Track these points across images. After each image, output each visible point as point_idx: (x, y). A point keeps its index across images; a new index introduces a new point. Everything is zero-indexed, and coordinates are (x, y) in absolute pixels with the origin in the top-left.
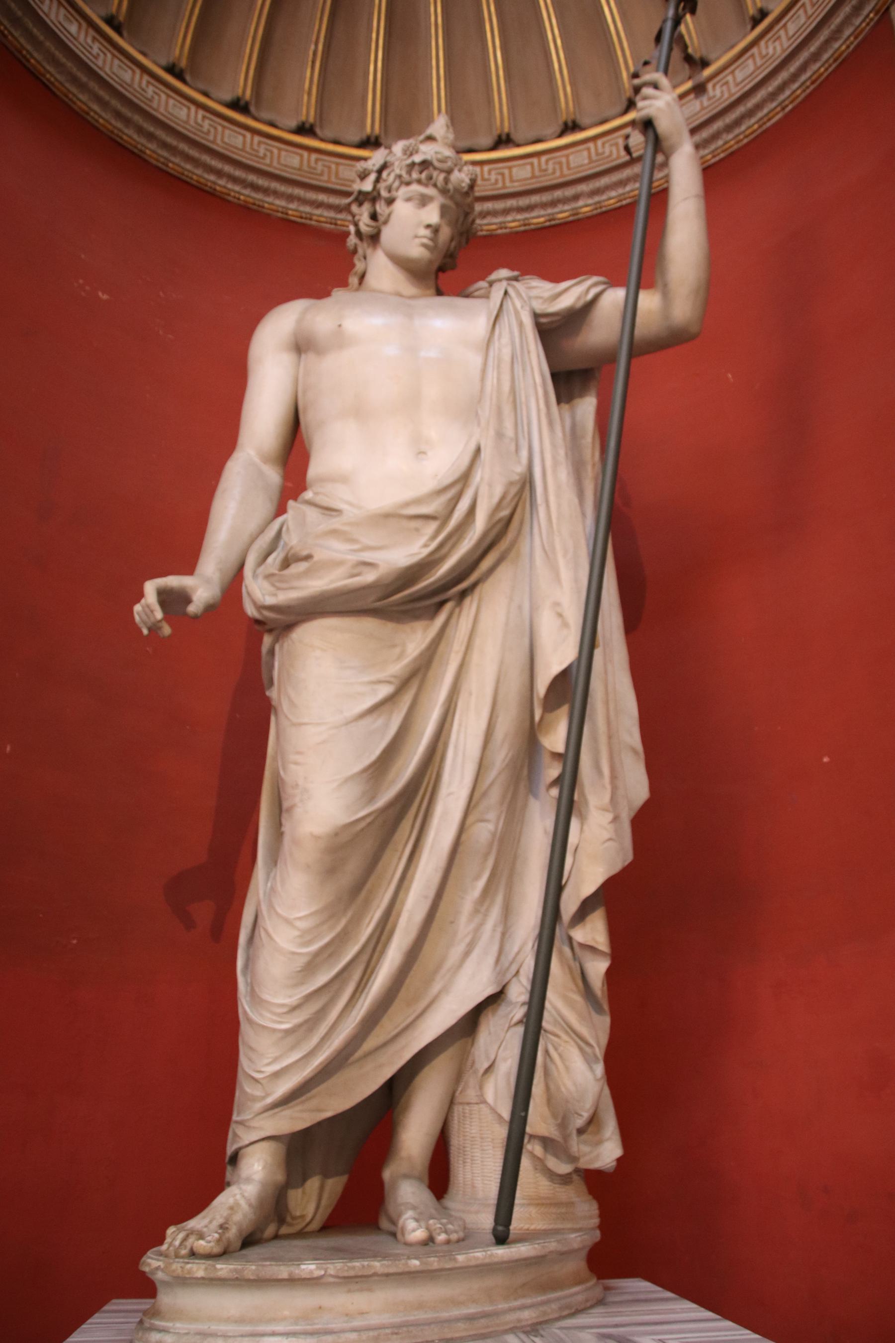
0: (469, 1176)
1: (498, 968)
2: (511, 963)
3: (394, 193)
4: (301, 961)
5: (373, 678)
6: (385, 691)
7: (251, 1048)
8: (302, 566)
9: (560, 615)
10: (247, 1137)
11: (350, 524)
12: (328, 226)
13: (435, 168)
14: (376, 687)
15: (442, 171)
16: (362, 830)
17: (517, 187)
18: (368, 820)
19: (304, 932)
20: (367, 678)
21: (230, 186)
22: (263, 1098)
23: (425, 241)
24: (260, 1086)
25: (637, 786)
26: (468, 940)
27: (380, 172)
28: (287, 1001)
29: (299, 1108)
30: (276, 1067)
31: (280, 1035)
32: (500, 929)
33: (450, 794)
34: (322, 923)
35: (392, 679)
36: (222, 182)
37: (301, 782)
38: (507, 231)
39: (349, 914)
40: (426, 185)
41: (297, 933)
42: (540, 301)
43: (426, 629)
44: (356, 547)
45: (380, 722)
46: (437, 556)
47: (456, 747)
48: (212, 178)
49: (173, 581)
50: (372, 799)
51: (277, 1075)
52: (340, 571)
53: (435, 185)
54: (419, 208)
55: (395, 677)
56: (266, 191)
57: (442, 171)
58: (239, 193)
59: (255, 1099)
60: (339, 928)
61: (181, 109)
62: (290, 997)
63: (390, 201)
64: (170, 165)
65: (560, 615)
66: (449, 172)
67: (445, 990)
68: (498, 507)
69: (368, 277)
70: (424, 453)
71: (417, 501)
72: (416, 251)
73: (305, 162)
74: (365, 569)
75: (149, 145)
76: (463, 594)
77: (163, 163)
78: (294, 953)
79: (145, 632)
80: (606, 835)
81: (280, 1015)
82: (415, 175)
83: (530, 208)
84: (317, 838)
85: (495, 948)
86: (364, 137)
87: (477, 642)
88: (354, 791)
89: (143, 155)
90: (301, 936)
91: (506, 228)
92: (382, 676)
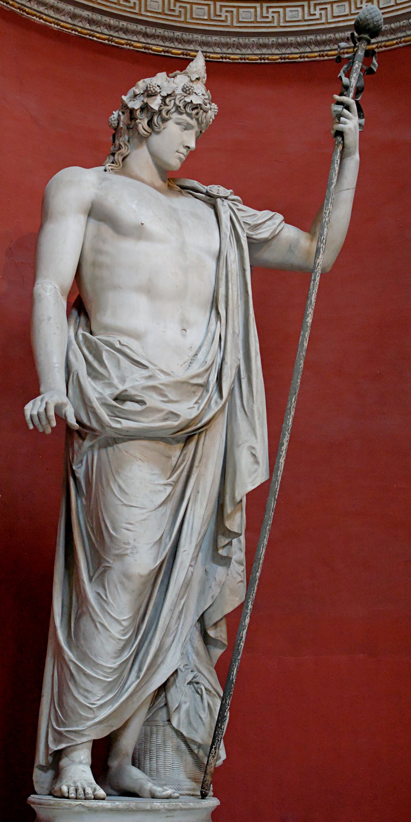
0: (154, 766)
4: (122, 643)
5: (166, 482)
7: (87, 691)
8: (137, 407)
9: (254, 455)
11: (162, 384)
13: (201, 109)
14: (166, 487)
19: (125, 628)
22: (94, 718)
23: (182, 156)
24: (92, 711)
26: (174, 634)
28: (114, 666)
30: (102, 702)
31: (106, 684)
33: (185, 551)
35: (171, 483)
37: (131, 542)
38: (131, 48)
40: (192, 118)
41: (122, 628)
42: (248, 227)
44: (165, 399)
53: (197, 120)
54: (183, 131)
55: (173, 481)
59: (88, 719)
62: (114, 663)
63: (164, 120)
65: (254, 455)
67: (162, 662)
69: (128, 159)
70: (185, 330)
72: (175, 162)
79: (31, 427)
80: (240, 579)
81: (108, 673)
82: (188, 110)
83: (153, 36)
84: (141, 576)
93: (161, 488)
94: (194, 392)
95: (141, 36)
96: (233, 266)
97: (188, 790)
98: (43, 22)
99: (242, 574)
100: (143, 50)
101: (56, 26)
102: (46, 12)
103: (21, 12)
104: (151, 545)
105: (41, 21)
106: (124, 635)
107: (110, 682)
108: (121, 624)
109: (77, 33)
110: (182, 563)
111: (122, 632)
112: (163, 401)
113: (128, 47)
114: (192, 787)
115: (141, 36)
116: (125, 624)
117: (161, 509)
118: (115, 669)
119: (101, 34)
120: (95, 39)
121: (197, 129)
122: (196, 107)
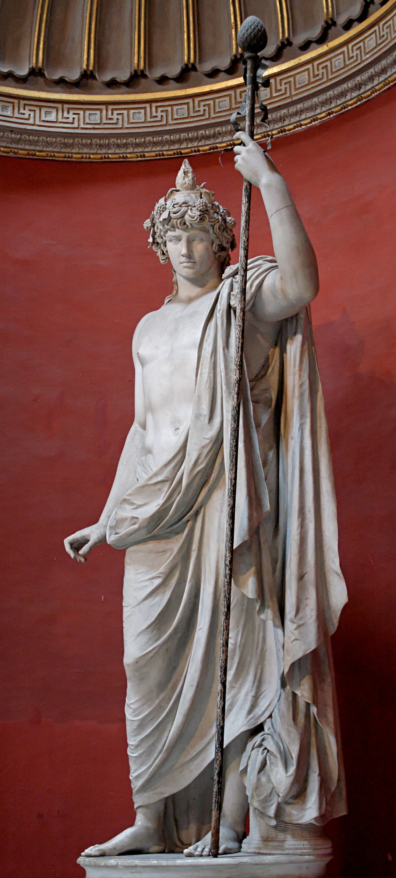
1: (251, 716)
2: (264, 712)
3: (164, 238)
4: (136, 724)
5: (150, 576)
6: (158, 581)
10: (135, 806)
11: (130, 495)
14: (153, 581)
15: (178, 219)
16: (152, 657)
17: (368, 59)
18: (154, 652)
19: (135, 710)
20: (147, 578)
21: (190, 145)
23: (185, 264)
25: (339, 595)
29: (151, 793)
30: (136, 774)
32: (252, 693)
34: (143, 705)
38: (378, 92)
39: (161, 697)
40: (174, 231)
41: (132, 711)
43: (177, 541)
44: (134, 507)
45: (157, 598)
46: (169, 503)
47: (202, 602)
48: (176, 146)
49: (78, 535)
50: (156, 641)
51: (137, 777)
52: (127, 523)
53: (178, 228)
56: (214, 136)
57: (178, 219)
58: (197, 146)
60: (154, 706)
61: (140, 113)
62: (135, 741)
63: (165, 244)
66: (183, 217)
71: (156, 475)
73: (233, 101)
74: (135, 520)
75: (128, 151)
76: (197, 513)
78: (132, 720)
84: (128, 665)
85: (247, 706)
86: (279, 44)
87: (205, 540)
88: (144, 638)
90: (134, 712)
91: (376, 91)
92: (154, 574)
93: (147, 583)
94: (160, 490)
95: (377, 78)
96: (207, 350)
97: (256, 848)
98: (305, 127)
99: (294, 632)
100: (386, 87)
101: (316, 122)
102: (303, 117)
103: (284, 133)
104: (134, 638)
105: (303, 127)
107: (136, 757)
108: (131, 708)
109: (334, 114)
110: (198, 640)
111: (133, 714)
112: (133, 509)
113: (376, 94)
114: (258, 846)
115: (377, 78)
118: (137, 746)
119: (351, 100)
120: (350, 108)
121: (185, 235)
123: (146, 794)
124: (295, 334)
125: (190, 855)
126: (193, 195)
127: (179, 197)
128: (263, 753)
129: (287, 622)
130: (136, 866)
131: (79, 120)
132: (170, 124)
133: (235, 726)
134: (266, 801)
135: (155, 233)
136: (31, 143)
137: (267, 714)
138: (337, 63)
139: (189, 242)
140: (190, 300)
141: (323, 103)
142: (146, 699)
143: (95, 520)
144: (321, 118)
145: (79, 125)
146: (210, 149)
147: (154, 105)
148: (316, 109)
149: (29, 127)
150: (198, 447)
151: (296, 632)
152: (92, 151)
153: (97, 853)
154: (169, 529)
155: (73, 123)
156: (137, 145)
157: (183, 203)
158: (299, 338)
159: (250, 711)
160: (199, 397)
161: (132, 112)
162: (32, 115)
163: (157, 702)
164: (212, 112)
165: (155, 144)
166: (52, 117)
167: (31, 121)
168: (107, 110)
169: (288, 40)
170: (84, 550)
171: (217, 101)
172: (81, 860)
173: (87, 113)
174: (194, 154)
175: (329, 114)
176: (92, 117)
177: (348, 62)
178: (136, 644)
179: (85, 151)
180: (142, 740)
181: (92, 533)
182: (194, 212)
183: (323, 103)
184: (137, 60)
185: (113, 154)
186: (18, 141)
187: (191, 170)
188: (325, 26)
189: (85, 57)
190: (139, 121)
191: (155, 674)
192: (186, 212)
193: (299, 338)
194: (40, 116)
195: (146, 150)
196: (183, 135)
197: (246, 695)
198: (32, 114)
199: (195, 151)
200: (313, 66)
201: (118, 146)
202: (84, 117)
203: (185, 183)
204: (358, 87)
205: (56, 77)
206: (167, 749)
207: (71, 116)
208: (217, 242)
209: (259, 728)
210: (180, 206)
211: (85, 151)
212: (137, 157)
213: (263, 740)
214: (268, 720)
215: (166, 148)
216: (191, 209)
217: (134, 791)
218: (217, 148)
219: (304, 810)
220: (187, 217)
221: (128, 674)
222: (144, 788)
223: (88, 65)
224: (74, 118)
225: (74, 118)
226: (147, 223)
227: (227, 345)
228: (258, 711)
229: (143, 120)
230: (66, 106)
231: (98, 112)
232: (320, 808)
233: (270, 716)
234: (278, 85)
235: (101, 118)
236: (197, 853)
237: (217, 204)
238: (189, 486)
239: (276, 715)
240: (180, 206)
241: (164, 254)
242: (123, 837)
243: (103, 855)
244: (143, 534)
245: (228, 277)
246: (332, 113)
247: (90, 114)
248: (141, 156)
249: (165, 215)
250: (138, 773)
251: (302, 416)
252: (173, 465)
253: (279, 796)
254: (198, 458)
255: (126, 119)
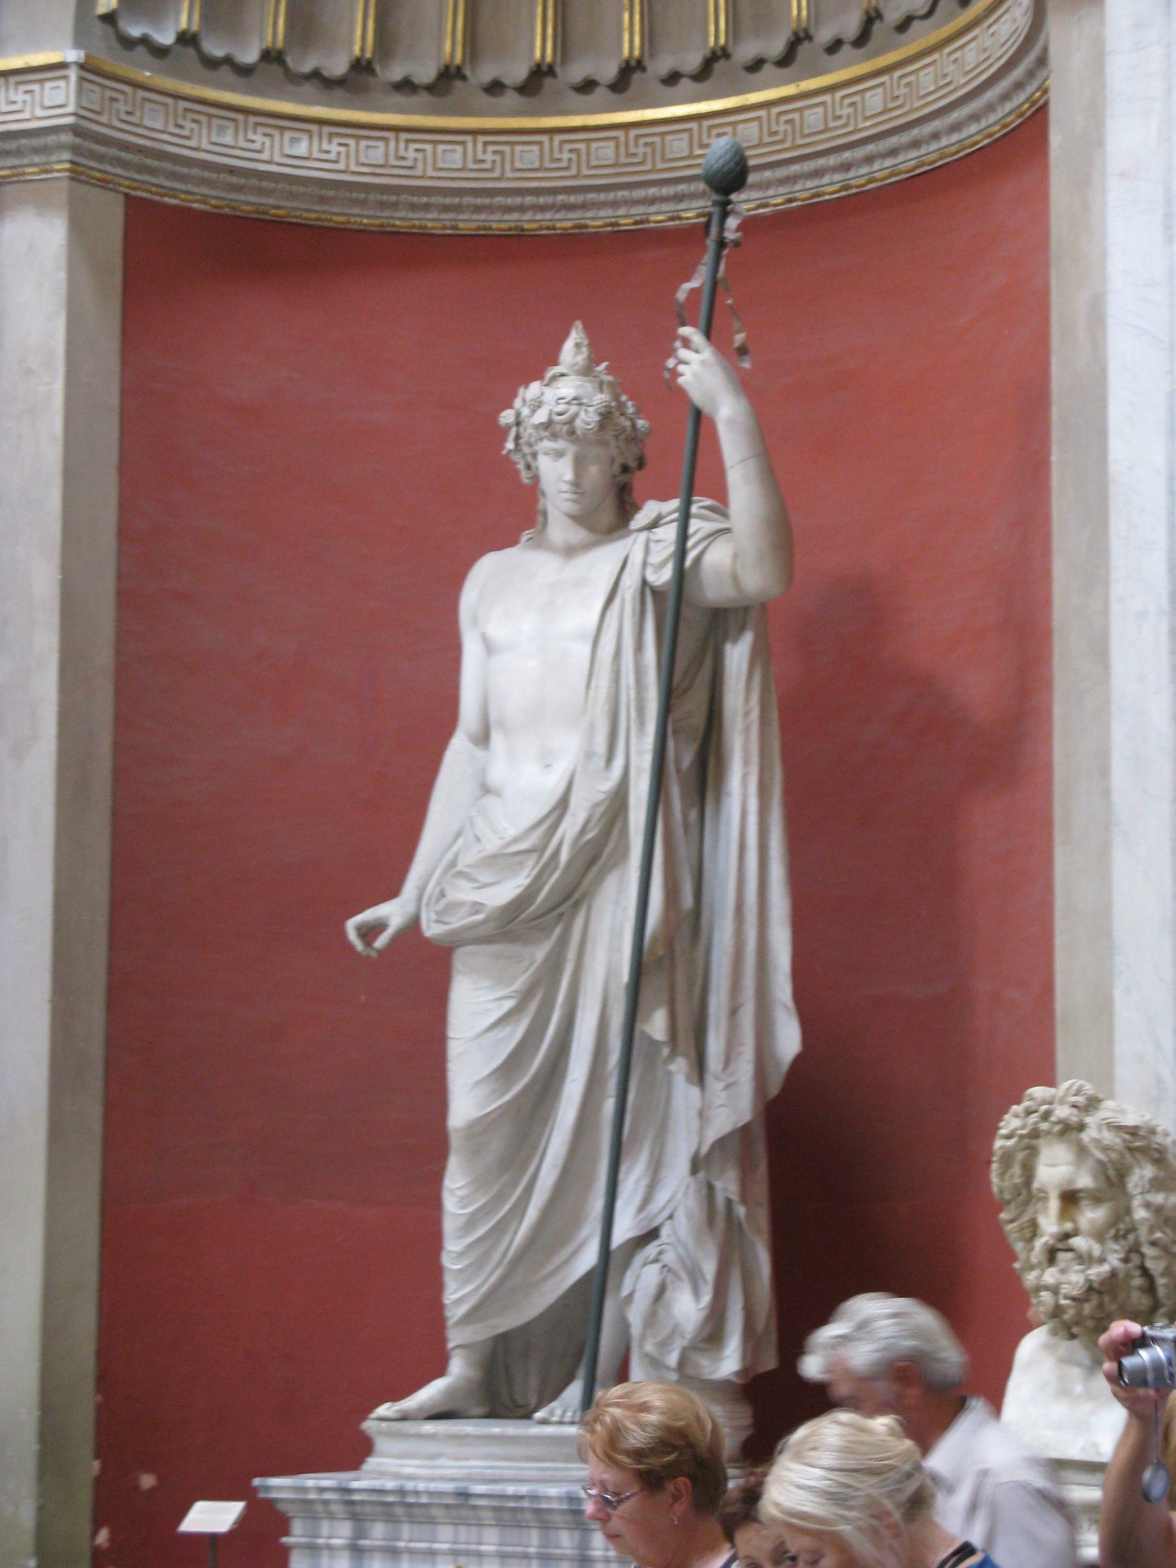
1: (642, 1215)
4: (462, 1220)
6: (509, 1004)
10: (451, 1345)
11: (468, 866)
12: (671, 223)
19: (462, 1199)
20: (490, 998)
21: (539, 217)
23: (568, 496)
25: (789, 1040)
27: (518, 424)
32: (644, 1182)
36: (527, 216)
48: (515, 216)
50: (503, 1094)
51: (459, 1301)
52: (463, 911)
56: (584, 206)
61: (454, 151)
63: (534, 455)
64: (461, 225)
66: (571, 422)
68: (584, 830)
71: (516, 840)
73: (622, 150)
75: (430, 216)
76: (576, 906)
77: (452, 228)
84: (457, 1130)
89: (426, 231)
93: (491, 1005)
94: (521, 863)
106: (464, 1207)
107: (460, 1271)
109: (799, 203)
116: (460, 1193)
117: (488, 1035)
118: (462, 1254)
119: (830, 186)
120: (827, 197)
121: (571, 449)
122: (548, 425)
123: (469, 1328)
124: (742, 630)
125: (544, 1422)
126: (588, 385)
127: (567, 388)
128: (661, 1273)
129: (709, 1079)
130: (466, 1436)
131: (348, 157)
132: (508, 179)
133: (623, 1230)
134: (664, 1344)
135: (518, 437)
136: (261, 192)
137: (666, 1213)
138: (812, 118)
139: (579, 464)
140: (570, 551)
141: (782, 181)
142: (479, 1183)
143: (392, 891)
144: (775, 205)
145: (348, 166)
146: (573, 228)
147: (481, 139)
148: (767, 188)
149: (263, 167)
150: (588, 804)
151: (723, 1095)
152: (366, 213)
153: (397, 1416)
154: (531, 924)
155: (336, 162)
156: (447, 208)
157: (575, 399)
158: (748, 639)
159: (642, 1207)
160: (592, 725)
161: (441, 148)
162: (268, 144)
163: (496, 1188)
164: (584, 165)
165: (478, 209)
166: (302, 149)
167: (265, 156)
168: (397, 141)
169: (724, 49)
170: (381, 942)
171: (594, 145)
172: (369, 1426)
173: (363, 143)
174: (544, 232)
175: (790, 201)
176: (371, 152)
177: (832, 124)
178: (467, 1099)
179: (356, 211)
180: (470, 1246)
181: (392, 913)
182: (591, 415)
183: (782, 181)
184: (451, 49)
185: (402, 219)
186: (240, 189)
187: (586, 342)
188: (792, 39)
189: (358, 33)
190: (454, 166)
191: (496, 1146)
192: (576, 415)
193: (748, 639)
194: (281, 147)
195: (461, 217)
196: (529, 200)
197: (637, 1183)
198: (267, 141)
199: (548, 228)
200: (769, 115)
201: (414, 207)
202: (357, 151)
203: (576, 364)
204: (846, 167)
205: (307, 68)
206: (509, 1263)
207: (334, 148)
208: (619, 460)
209: (652, 1234)
210: (568, 403)
211: (356, 211)
212: (444, 228)
213: (661, 1253)
214: (668, 1222)
215: (497, 217)
216: (586, 411)
217: (450, 1323)
218: (586, 226)
219: (718, 1359)
220: (578, 423)
221: (455, 1141)
222: (468, 1319)
223: (363, 49)
224: (339, 153)
225: (339, 153)
226: (507, 417)
227: (639, 647)
228: (654, 1207)
229: (459, 165)
230: (327, 129)
231: (381, 144)
232: (744, 1357)
233: (671, 1217)
234: (705, 136)
235: (387, 155)
236: (555, 1419)
237: (624, 398)
238: (570, 862)
239: (681, 1215)
240: (568, 403)
241: (529, 467)
242: (430, 1393)
243: (404, 1417)
244: (490, 928)
245: (641, 530)
246: (795, 200)
247: (368, 147)
248: (452, 228)
249: (541, 417)
250: (458, 1296)
251: (746, 762)
252: (544, 827)
253: (683, 1338)
254: (588, 821)
255: (430, 161)
